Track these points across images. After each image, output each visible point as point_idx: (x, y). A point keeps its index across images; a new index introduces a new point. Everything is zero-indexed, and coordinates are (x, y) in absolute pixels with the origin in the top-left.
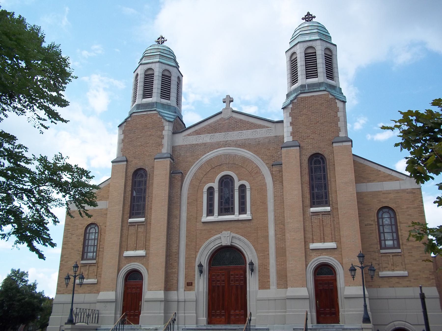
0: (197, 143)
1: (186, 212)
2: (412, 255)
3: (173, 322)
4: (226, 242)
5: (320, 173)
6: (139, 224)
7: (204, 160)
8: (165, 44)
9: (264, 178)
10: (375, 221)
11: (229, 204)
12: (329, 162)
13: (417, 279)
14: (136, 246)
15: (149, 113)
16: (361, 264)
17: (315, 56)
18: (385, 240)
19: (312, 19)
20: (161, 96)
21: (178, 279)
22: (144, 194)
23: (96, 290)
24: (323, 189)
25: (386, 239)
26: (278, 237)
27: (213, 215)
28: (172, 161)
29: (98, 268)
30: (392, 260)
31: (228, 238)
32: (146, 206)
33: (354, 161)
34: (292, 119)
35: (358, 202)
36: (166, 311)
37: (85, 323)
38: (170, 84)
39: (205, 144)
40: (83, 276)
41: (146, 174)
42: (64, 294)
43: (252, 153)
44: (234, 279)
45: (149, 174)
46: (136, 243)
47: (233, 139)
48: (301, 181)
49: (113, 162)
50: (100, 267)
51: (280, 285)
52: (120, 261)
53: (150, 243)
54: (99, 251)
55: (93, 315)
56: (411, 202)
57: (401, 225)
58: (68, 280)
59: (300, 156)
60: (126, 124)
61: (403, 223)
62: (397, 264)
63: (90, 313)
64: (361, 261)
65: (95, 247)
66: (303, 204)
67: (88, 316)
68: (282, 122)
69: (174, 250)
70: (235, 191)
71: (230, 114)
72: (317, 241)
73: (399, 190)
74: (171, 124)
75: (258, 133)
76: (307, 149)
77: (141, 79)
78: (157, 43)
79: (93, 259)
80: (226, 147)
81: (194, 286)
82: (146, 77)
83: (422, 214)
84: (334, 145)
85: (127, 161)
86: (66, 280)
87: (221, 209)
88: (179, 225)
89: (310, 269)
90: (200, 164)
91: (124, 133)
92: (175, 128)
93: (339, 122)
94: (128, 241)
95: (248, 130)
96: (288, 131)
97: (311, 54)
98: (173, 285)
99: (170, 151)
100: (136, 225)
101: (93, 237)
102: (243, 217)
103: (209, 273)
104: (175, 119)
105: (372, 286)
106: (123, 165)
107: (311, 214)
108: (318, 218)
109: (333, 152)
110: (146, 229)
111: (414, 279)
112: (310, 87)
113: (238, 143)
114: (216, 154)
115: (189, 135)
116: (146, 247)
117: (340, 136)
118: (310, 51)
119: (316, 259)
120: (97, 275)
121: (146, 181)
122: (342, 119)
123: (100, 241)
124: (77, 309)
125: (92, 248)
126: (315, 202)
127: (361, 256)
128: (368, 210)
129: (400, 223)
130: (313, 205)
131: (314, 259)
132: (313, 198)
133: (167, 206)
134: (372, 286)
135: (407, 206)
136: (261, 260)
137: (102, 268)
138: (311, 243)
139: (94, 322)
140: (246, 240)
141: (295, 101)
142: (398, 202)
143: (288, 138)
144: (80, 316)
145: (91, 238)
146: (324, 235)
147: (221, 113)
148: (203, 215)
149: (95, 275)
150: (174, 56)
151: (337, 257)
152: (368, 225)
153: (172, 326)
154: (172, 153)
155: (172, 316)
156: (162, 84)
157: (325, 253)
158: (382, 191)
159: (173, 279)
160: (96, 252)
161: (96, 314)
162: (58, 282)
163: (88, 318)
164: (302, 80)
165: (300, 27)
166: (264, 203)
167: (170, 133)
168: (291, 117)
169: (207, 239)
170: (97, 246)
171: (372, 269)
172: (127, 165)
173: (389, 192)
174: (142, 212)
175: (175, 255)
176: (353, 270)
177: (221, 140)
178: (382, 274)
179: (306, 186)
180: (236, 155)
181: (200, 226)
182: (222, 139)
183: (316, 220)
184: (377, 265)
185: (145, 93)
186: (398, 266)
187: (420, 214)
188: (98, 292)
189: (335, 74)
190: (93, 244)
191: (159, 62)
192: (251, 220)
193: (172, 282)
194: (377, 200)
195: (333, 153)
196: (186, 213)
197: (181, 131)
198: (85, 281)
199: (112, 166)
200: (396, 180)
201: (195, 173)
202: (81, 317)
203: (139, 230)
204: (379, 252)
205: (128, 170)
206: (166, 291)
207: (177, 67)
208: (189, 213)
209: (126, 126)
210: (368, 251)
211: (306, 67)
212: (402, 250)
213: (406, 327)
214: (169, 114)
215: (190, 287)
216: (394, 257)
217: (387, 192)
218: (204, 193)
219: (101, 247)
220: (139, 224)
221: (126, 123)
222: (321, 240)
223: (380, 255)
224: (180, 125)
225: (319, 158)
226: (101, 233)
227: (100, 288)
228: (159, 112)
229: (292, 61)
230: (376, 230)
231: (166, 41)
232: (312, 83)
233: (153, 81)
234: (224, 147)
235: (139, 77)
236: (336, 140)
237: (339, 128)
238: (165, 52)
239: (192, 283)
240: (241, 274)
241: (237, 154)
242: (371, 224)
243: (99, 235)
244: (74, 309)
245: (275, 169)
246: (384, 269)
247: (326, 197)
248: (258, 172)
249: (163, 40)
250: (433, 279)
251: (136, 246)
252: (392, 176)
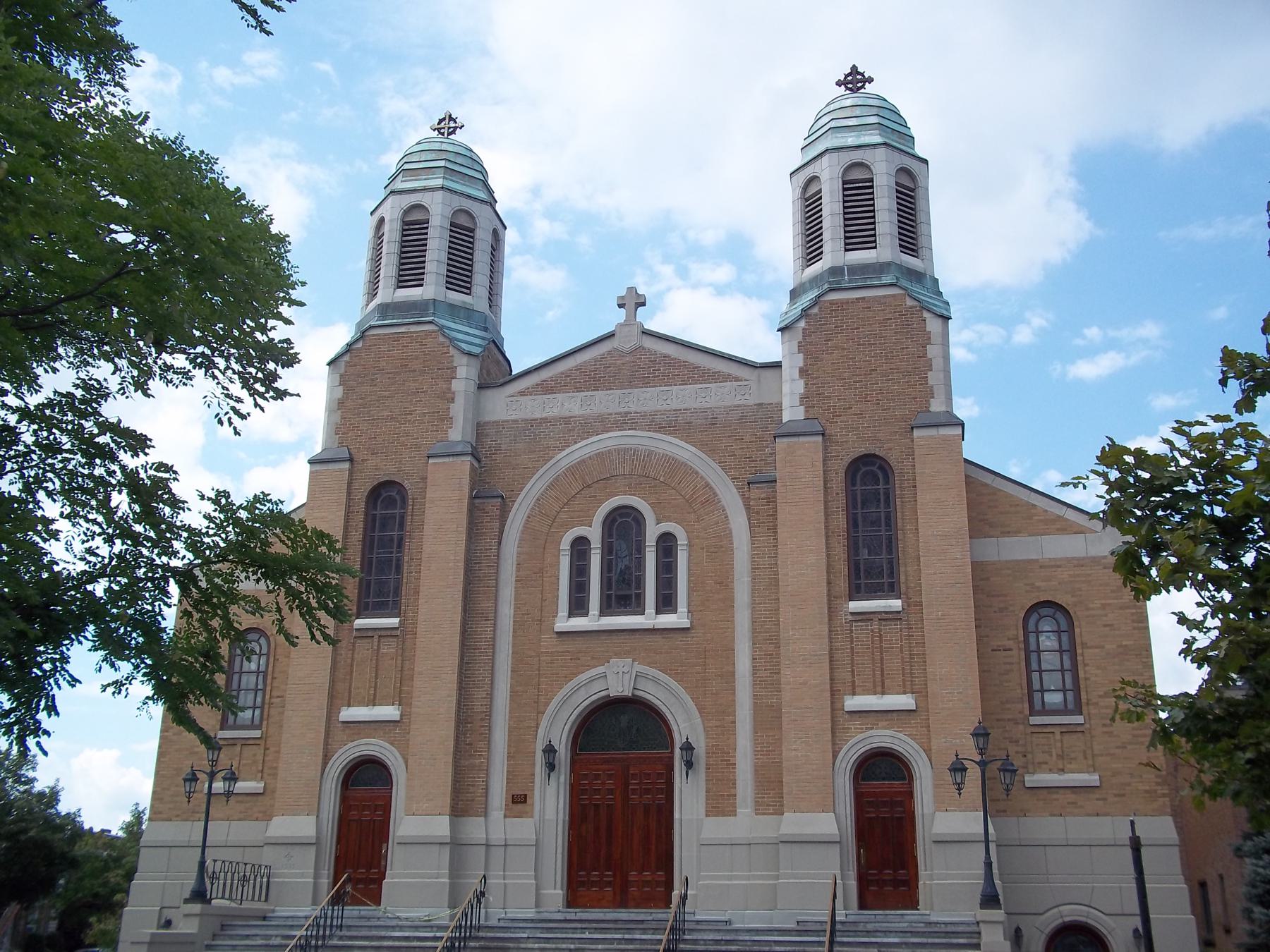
0: (544, 415)
1: (513, 603)
2: (1112, 732)
3: (479, 901)
4: (620, 688)
5: (877, 508)
6: (383, 633)
7: (564, 463)
8: (459, 136)
9: (726, 517)
10: (1017, 639)
11: (629, 585)
12: (901, 480)
13: (1123, 795)
14: (375, 694)
15: (413, 328)
16: (981, 754)
17: (871, 190)
18: (1042, 691)
19: (864, 85)
20: (447, 282)
21: (487, 785)
22: (398, 553)
23: (260, 812)
24: (884, 551)
25: (1045, 688)
26: (759, 677)
27: (586, 614)
28: (476, 465)
29: (268, 752)
30: (1059, 745)
31: (627, 676)
32: (404, 585)
33: (967, 476)
34: (804, 359)
35: (976, 589)
36: (456, 871)
37: (230, 899)
38: (471, 251)
39: (566, 420)
40: (233, 773)
41: (404, 497)
42: (171, 820)
43: (693, 449)
44: (641, 788)
45: (413, 499)
46: (373, 685)
47: (645, 409)
48: (827, 527)
49: (311, 462)
50: (272, 749)
52: (328, 734)
53: (412, 686)
54: (270, 704)
55: (255, 880)
56: (1113, 591)
57: (1087, 652)
58: (193, 784)
59: (824, 461)
60: (351, 357)
61: (1091, 647)
62: (1073, 755)
63: (248, 874)
64: (981, 746)
65: (260, 694)
66: (829, 590)
67: (244, 880)
68: (776, 366)
69: (478, 707)
70: (647, 549)
71: (634, 340)
72: (864, 690)
73: (1084, 558)
74: (476, 363)
75: (713, 394)
76: (841, 442)
77: (392, 233)
78: (436, 132)
79: (252, 726)
80: (625, 430)
82: (407, 227)
83: (1140, 625)
84: (916, 433)
85: (351, 460)
86: (188, 784)
87: (609, 597)
88: (494, 638)
89: (844, 765)
90: (551, 473)
91: (343, 381)
92: (484, 371)
93: (930, 373)
94: (351, 679)
95: (686, 384)
96: (792, 393)
97: (861, 185)
98: (473, 800)
99: (471, 437)
100: (376, 637)
101: (253, 666)
102: (667, 620)
103: (573, 770)
104: (485, 348)
105: (1005, 811)
106: (341, 470)
107: (850, 617)
108: (868, 630)
109: (913, 451)
110: (403, 650)
111: (1116, 795)
112: (854, 274)
113: (658, 419)
114: (595, 447)
115: (522, 393)
116: (401, 699)
117: (933, 409)
118: (857, 175)
119: (860, 737)
120: (266, 771)
121: (402, 517)
122: (937, 364)
123: (273, 678)
124: (215, 861)
125: (251, 696)
126: (863, 586)
127: (981, 734)
128: (1001, 610)
129: (1084, 645)
130: (856, 592)
131: (854, 737)
132: (858, 576)
133: (461, 587)
134: (1005, 811)
135: (1103, 602)
136: (714, 738)
137: (278, 752)
138: (849, 694)
139: (256, 898)
140: (674, 684)
141: (815, 310)
142: (1080, 590)
143: (792, 412)
144: (221, 882)
145: (247, 670)
146: (882, 675)
147: (611, 336)
148: (560, 614)
149: (258, 771)
150: (484, 172)
151: (917, 735)
152: (1000, 650)
153: (474, 910)
154: (476, 442)
155: (474, 883)
156: (451, 251)
157: (885, 723)
158: (1037, 561)
159: (473, 786)
160: (262, 708)
161: (262, 878)
162: (154, 788)
163: (243, 886)
164: (833, 254)
165: (832, 107)
166: (725, 583)
167: (472, 387)
168: (801, 354)
169: (568, 679)
170: (264, 690)
171: (1008, 769)
172: (351, 472)
173: (1058, 563)
174: (391, 603)
175: (482, 720)
176: (958, 768)
177: (610, 411)
178: (1032, 780)
179: (839, 543)
180: (650, 453)
181: (547, 641)
182: (614, 408)
183: (863, 633)
184: (1020, 755)
185: (401, 273)
186: (1075, 759)
187: (1135, 625)
188: (268, 817)
189: (922, 241)
190: (252, 686)
191: (442, 188)
192: (688, 629)
193: (471, 793)
194: (1026, 585)
195: (911, 454)
196: (512, 607)
197: (502, 381)
198: (241, 786)
199: (311, 472)
200: (1075, 533)
201: (538, 499)
202: (224, 884)
203: (384, 649)
204: (1027, 722)
205: (356, 485)
206: (456, 816)
207: (491, 202)
209: (348, 364)
210: (998, 720)
211: (845, 219)
212: (1087, 718)
213: (1090, 921)
214: (469, 334)
215: (520, 806)
216: (1066, 737)
217: (1053, 563)
218: (562, 553)
219: (275, 693)
220: (383, 633)
221: (349, 354)
222: (875, 687)
223: (1029, 730)
224: (498, 362)
225: (875, 468)
226: (277, 657)
227: (273, 806)
228: (442, 328)
229: (807, 200)
230: (1019, 663)
231: (461, 128)
232: (861, 262)
233: (426, 239)
234: (619, 430)
235: (386, 228)
236: (922, 419)
237: (928, 387)
238: (460, 160)
239: (525, 796)
240: (659, 774)
241: (652, 449)
242: (1007, 647)
243: (271, 660)
244: (209, 862)
245: (757, 493)
246: (1039, 766)
247: (892, 573)
248: (711, 500)
249: (452, 124)
250: (1164, 795)
251: (375, 694)
252: (1067, 520)
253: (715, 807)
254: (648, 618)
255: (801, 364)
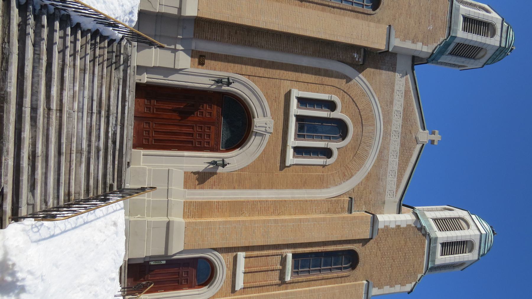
0: (395, 91)
9: (336, 185)
26: (257, 204)
39: (391, 103)
43: (369, 169)
51: (189, 206)
81: (198, 68)
93: (389, 287)
98: (204, 31)
102: (290, 152)
131: (224, 258)
151: (222, 291)
166: (304, 184)
169: (266, 95)
175: (249, 42)
208: (305, 69)
234: (383, 130)
237: (383, 287)
253: (189, 178)
254: (292, 141)
255: (402, 226)
